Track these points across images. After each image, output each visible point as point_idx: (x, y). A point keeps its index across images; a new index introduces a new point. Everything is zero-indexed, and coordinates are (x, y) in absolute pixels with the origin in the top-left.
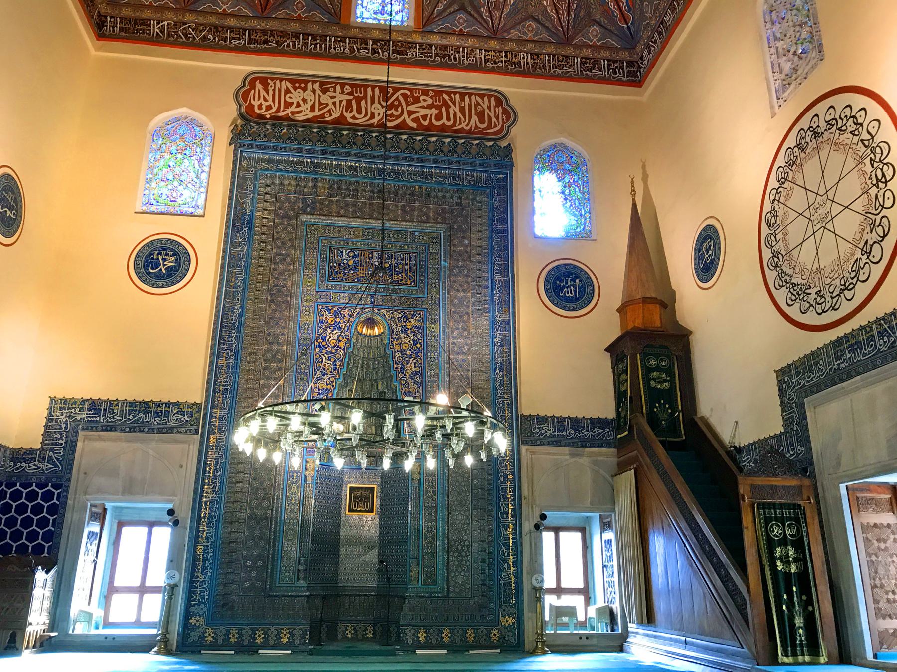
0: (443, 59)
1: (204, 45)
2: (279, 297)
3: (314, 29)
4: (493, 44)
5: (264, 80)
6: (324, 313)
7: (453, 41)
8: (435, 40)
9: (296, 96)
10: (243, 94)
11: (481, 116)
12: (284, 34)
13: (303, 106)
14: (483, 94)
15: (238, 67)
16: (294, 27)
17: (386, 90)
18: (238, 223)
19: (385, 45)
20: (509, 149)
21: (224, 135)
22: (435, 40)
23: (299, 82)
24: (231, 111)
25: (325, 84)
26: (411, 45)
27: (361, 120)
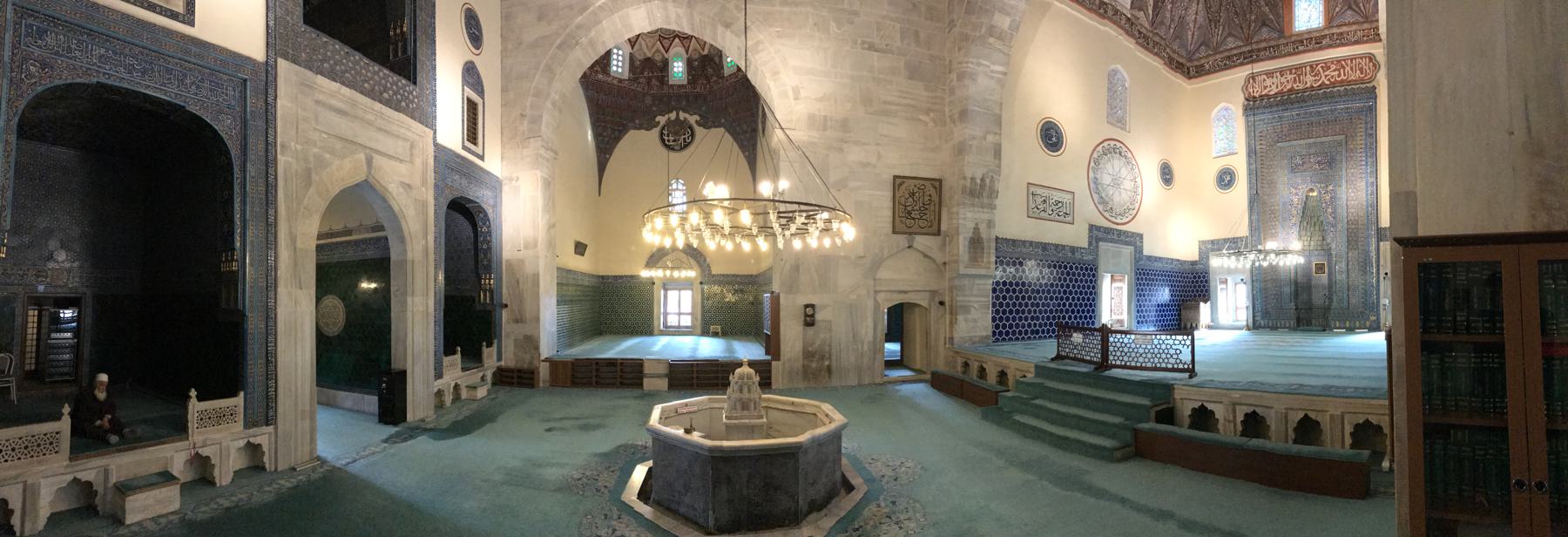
0: (1341, 41)
1: (1227, 67)
2: (1272, 184)
3: (1272, 43)
4: (1366, 26)
5: (1253, 77)
6: (1293, 190)
7: (1344, 29)
8: (1335, 30)
9: (1268, 82)
10: (1245, 88)
11: (1361, 70)
12: (1259, 50)
13: (1273, 86)
14: (1361, 57)
15: (1242, 73)
16: (1263, 45)
17: (1312, 66)
18: (1251, 153)
19: (1314, 40)
20: (1374, 88)
21: (1240, 111)
22: (1335, 30)
23: (1270, 74)
24: (1241, 99)
25: (1282, 72)
26: (1324, 37)
27: (1301, 87)
